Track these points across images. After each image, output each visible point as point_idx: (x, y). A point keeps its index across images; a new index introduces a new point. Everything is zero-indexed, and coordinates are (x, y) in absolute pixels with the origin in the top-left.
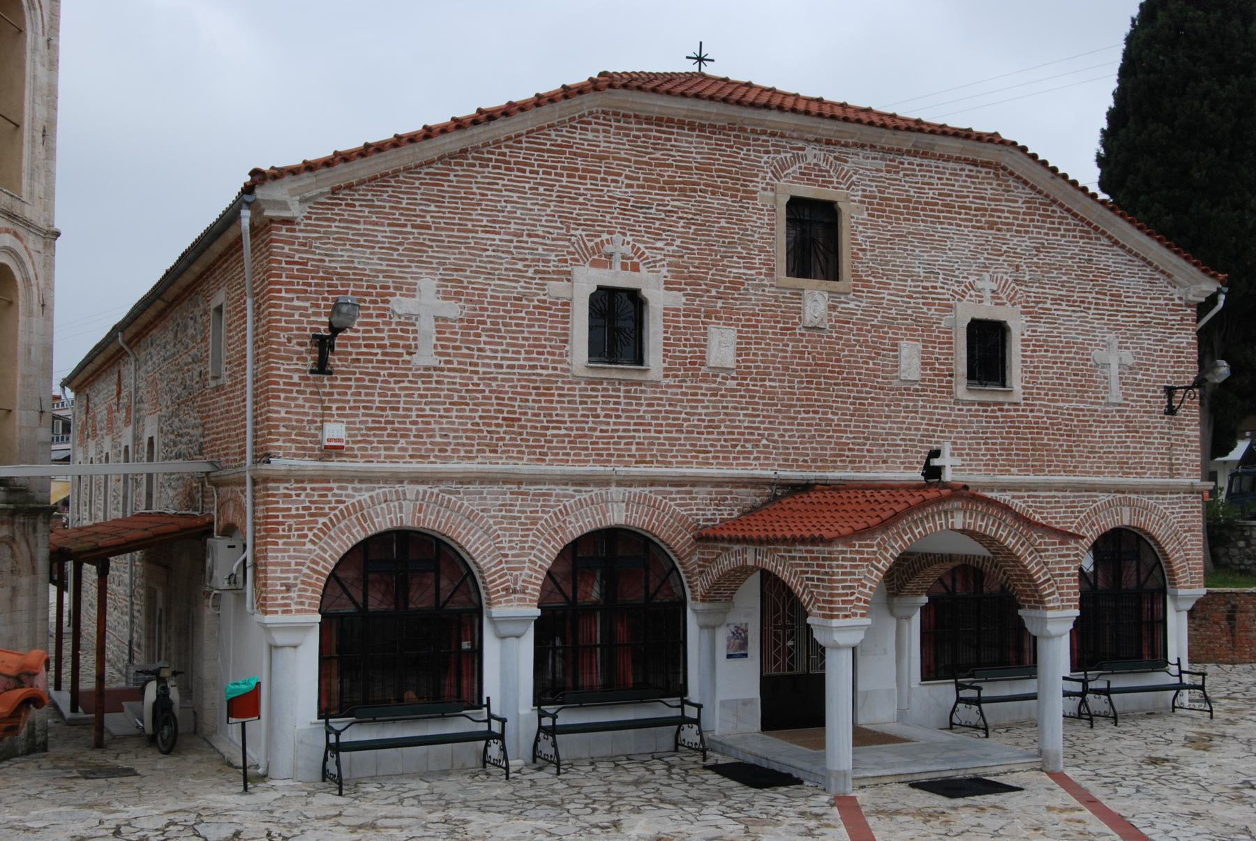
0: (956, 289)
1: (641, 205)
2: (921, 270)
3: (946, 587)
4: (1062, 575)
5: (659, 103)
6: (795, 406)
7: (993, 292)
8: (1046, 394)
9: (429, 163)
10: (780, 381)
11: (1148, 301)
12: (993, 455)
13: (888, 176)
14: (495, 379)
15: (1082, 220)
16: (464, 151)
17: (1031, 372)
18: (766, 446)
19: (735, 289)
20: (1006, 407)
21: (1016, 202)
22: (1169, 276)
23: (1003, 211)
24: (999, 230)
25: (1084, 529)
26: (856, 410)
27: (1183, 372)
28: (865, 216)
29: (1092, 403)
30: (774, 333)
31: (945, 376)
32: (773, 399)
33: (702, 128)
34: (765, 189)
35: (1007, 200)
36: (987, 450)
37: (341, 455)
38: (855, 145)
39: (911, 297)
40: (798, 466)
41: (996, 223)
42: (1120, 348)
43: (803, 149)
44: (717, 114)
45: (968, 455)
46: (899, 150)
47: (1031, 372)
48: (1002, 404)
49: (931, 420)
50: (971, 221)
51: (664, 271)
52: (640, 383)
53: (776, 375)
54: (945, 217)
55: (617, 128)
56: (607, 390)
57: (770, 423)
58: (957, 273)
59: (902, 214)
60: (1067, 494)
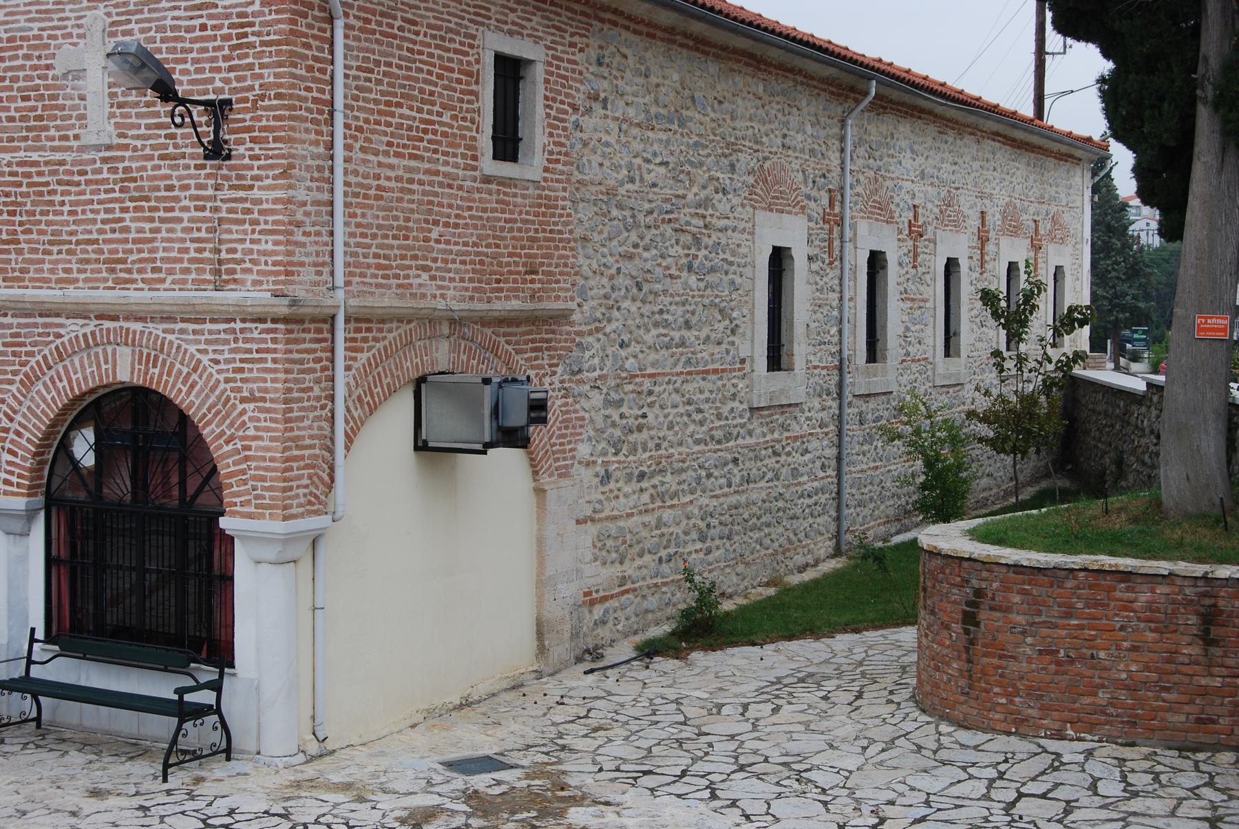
25: (40, 386)
27: (250, 67)
29: (54, 149)
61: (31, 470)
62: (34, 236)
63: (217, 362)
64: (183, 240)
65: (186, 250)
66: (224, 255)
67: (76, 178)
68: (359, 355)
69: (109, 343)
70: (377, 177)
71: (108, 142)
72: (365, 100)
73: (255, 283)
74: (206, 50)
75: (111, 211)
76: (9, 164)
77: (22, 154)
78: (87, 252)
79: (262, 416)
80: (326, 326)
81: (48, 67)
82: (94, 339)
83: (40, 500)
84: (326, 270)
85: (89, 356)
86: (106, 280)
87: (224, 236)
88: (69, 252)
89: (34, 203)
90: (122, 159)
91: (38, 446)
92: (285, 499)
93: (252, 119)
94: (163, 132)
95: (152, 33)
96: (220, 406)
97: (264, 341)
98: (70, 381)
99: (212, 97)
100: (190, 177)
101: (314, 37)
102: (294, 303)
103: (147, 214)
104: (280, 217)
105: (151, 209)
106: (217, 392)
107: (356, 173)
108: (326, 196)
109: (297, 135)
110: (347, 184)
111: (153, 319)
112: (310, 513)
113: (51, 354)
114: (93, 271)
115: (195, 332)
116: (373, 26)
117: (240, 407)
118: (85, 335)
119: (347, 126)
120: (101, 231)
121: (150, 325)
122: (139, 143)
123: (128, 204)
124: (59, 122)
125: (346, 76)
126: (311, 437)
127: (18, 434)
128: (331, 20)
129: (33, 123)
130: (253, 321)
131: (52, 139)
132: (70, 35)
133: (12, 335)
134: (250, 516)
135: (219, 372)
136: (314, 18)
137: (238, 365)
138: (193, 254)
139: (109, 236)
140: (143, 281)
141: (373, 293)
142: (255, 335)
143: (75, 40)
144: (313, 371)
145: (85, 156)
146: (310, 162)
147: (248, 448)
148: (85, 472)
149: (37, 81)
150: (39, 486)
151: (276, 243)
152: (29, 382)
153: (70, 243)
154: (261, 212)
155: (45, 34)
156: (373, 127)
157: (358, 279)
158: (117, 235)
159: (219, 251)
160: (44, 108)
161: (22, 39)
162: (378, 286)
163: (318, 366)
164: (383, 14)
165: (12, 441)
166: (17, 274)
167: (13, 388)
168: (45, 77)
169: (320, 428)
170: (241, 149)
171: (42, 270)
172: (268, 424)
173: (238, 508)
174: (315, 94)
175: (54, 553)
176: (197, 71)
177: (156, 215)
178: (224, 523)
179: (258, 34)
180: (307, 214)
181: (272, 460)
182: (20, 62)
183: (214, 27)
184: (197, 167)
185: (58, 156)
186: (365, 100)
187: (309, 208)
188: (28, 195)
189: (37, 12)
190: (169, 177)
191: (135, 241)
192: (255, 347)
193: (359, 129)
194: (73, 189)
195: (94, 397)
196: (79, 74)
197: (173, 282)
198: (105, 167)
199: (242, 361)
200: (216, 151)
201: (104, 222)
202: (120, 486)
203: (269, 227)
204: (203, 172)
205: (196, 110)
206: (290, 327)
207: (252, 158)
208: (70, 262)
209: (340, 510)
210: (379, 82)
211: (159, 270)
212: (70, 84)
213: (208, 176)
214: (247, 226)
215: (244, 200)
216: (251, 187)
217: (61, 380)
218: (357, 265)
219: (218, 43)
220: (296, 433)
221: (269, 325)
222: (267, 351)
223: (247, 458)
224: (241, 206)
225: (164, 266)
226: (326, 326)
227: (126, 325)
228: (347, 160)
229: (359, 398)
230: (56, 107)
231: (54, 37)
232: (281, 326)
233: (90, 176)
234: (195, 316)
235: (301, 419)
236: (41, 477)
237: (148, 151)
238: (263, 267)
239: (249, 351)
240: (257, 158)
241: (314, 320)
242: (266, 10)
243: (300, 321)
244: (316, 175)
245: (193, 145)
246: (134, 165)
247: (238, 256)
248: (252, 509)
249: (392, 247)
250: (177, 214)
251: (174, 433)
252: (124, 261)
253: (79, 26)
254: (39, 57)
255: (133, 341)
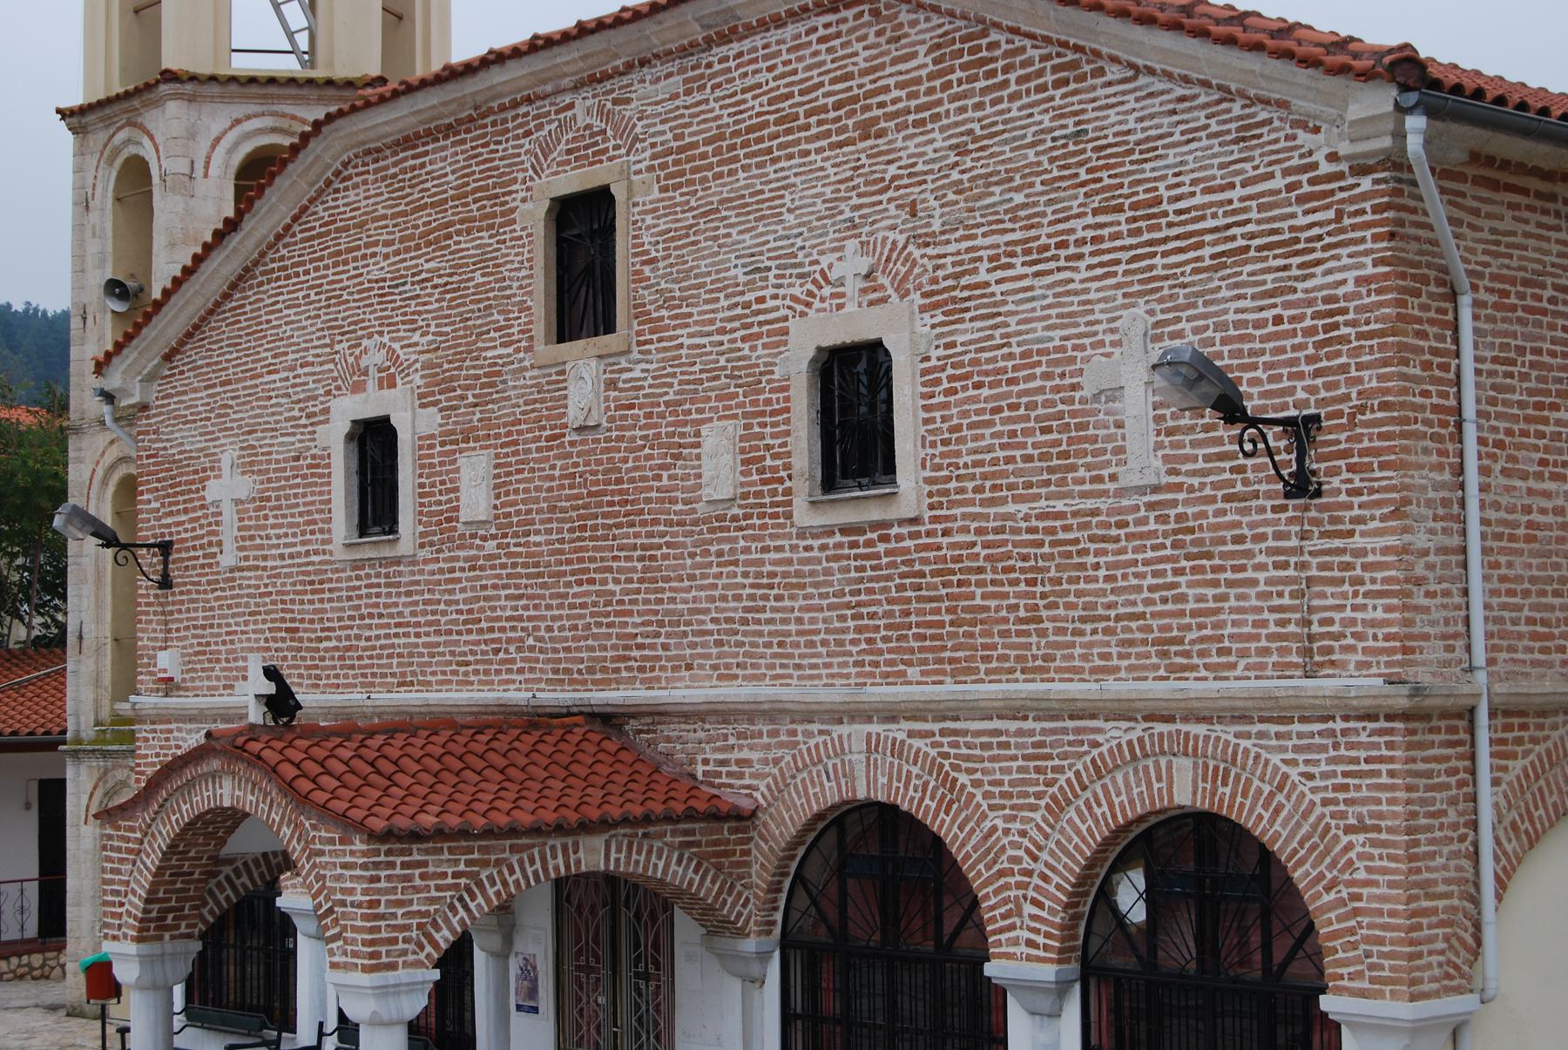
0: (797, 291)
1: (398, 281)
2: (740, 271)
3: (830, 928)
4: (343, 903)
5: (380, 120)
6: (564, 573)
7: (867, 276)
8: (977, 490)
9: (227, 296)
10: (549, 531)
11: (1239, 192)
12: (869, 641)
13: (690, 100)
14: (278, 576)
15: (1047, 40)
16: (247, 270)
17: (945, 442)
18: (532, 649)
19: (492, 385)
20: (895, 530)
21: (914, 55)
22: (1282, 104)
23: (886, 89)
24: (880, 134)
26: (645, 570)
27: (1344, 369)
28: (656, 194)
29: (1084, 495)
30: (539, 450)
31: (781, 481)
32: (536, 565)
33: (448, 130)
34: (524, 200)
35: (894, 62)
36: (859, 630)
37: (179, 688)
38: (629, 67)
39: (722, 331)
40: (572, 682)
41: (876, 120)
42: (1157, 338)
43: (571, 106)
44: (444, 104)
45: (824, 643)
46: (691, 45)
47: (942, 440)
48: (886, 525)
49: (759, 575)
50: (828, 134)
51: (417, 379)
52: (397, 561)
53: (542, 522)
54: (781, 147)
55: (376, 171)
56: (368, 576)
57: (536, 607)
58: (801, 254)
59: (710, 167)
60: (1029, 724)
61: (1062, 927)
62: (1061, 612)
63: (1310, 777)
64: (1259, 610)
65: (1263, 624)
66: (1315, 628)
67: (1114, 532)
68: (1511, 763)
69: (1163, 753)
70: (1528, 510)
71: (1154, 481)
72: (1505, 403)
73: (1361, 665)
74: (1282, 350)
75: (1162, 573)
76: (1026, 518)
77: (1043, 503)
78: (1130, 630)
79: (1376, 852)
80: (1462, 724)
81: (1074, 387)
82: (1143, 748)
83: (1074, 967)
84: (1459, 644)
85: (1136, 771)
86: (1156, 667)
87: (1315, 602)
88: (1106, 631)
89: (1059, 568)
90: (1174, 503)
91: (1070, 895)
92: (1411, 970)
93: (1348, 440)
94: (1228, 465)
95: (1209, 333)
96: (1316, 839)
97: (1376, 746)
98: (1111, 806)
99: (1293, 413)
100: (1266, 523)
101: (1432, 322)
102: (1417, 691)
103: (1210, 576)
104: (1393, 573)
105: (1215, 569)
106: (1312, 819)
107: (1496, 506)
108: (1456, 541)
109: (1412, 458)
110: (1485, 522)
111: (1221, 720)
112: (1449, 991)
113: (1086, 768)
114: (1138, 656)
115: (1278, 736)
116: (1513, 300)
117: (1345, 840)
118: (1130, 743)
119: (1482, 441)
120: (1148, 602)
121: (1217, 727)
122: (1195, 481)
123: (1184, 563)
124: (1089, 459)
125: (1478, 372)
126: (1447, 881)
127: (1045, 878)
128: (1453, 296)
129: (1055, 462)
130: (1360, 718)
131: (1082, 481)
132: (1102, 344)
133: (1035, 745)
134: (1363, 994)
135: (1314, 790)
136: (1431, 295)
137: (1340, 780)
138: (1273, 629)
139: (1159, 607)
140: (1207, 667)
141: (1527, 675)
142: (1363, 738)
143: (1108, 349)
144: (1445, 787)
145: (1125, 502)
146: (1431, 494)
147: (1358, 897)
148: (1133, 930)
149: (1061, 407)
150: (1072, 949)
151: (1388, 609)
152: (1057, 808)
153: (1108, 618)
154: (1365, 567)
155: (1069, 344)
156: (1518, 440)
157: (1504, 655)
158: (1169, 607)
159: (1309, 623)
160: (1070, 441)
161: (1040, 352)
162: (1534, 663)
163: (1453, 780)
164: (1526, 283)
165: (1037, 888)
166: (1039, 663)
167: (1037, 816)
168: (1071, 401)
169: (1459, 869)
170: (1336, 482)
171: (1072, 657)
172: (1385, 863)
173: (1345, 983)
174: (1435, 400)
175: (1094, 1041)
176: (1271, 379)
177: (1222, 576)
178: (1327, 1003)
179: (1354, 324)
180: (1430, 567)
181: (1392, 914)
182: (1038, 383)
183: (1292, 319)
184: (1275, 509)
185: (1090, 504)
186: (1505, 403)
187: (1432, 558)
188: (1051, 557)
189: (1058, 316)
190: (1238, 525)
191: (1194, 614)
192: (1363, 754)
193: (1499, 444)
194: (1110, 546)
195: (1144, 826)
196: (1114, 394)
197: (1247, 668)
198: (1152, 515)
199: (1345, 774)
200: (1301, 486)
201: (1151, 589)
202: (1180, 949)
203: (1377, 587)
204: (1283, 516)
205: (1271, 433)
206: (1412, 725)
207: (1350, 493)
208: (1108, 644)
209: (1491, 985)
210: (1524, 377)
211: (1228, 651)
212: (1102, 407)
213: (1290, 521)
214: (1346, 587)
215: (1342, 551)
216: (1351, 533)
217: (1099, 805)
218: (1503, 635)
219: (1299, 340)
220: (1426, 875)
221: (1382, 724)
222: (1381, 760)
223: (1356, 912)
224: (1337, 559)
225: (1235, 646)
226: (1462, 724)
227: (1185, 728)
228: (1484, 488)
229: (1514, 825)
230: (1086, 439)
231: (1082, 348)
232: (1399, 725)
233: (1132, 529)
234: (1279, 713)
235: (1431, 856)
236: (1074, 937)
237: (1208, 491)
238: (1371, 643)
239: (1356, 761)
240: (1357, 492)
241: (1445, 715)
242: (1364, 291)
243: (1425, 716)
244: (1441, 511)
245: (1269, 480)
246: (1190, 511)
247: (1335, 628)
248: (1366, 985)
249: (1552, 608)
250: (1249, 574)
251: (1253, 877)
252: (1180, 641)
253: (1112, 331)
254: (1063, 375)
255: (1195, 749)
